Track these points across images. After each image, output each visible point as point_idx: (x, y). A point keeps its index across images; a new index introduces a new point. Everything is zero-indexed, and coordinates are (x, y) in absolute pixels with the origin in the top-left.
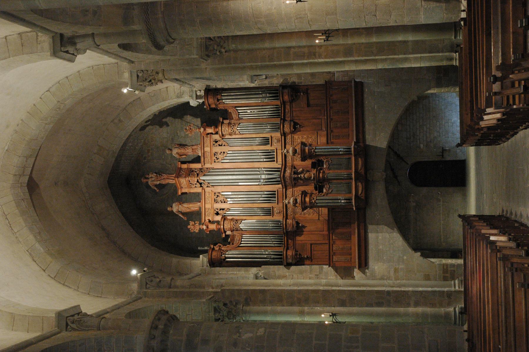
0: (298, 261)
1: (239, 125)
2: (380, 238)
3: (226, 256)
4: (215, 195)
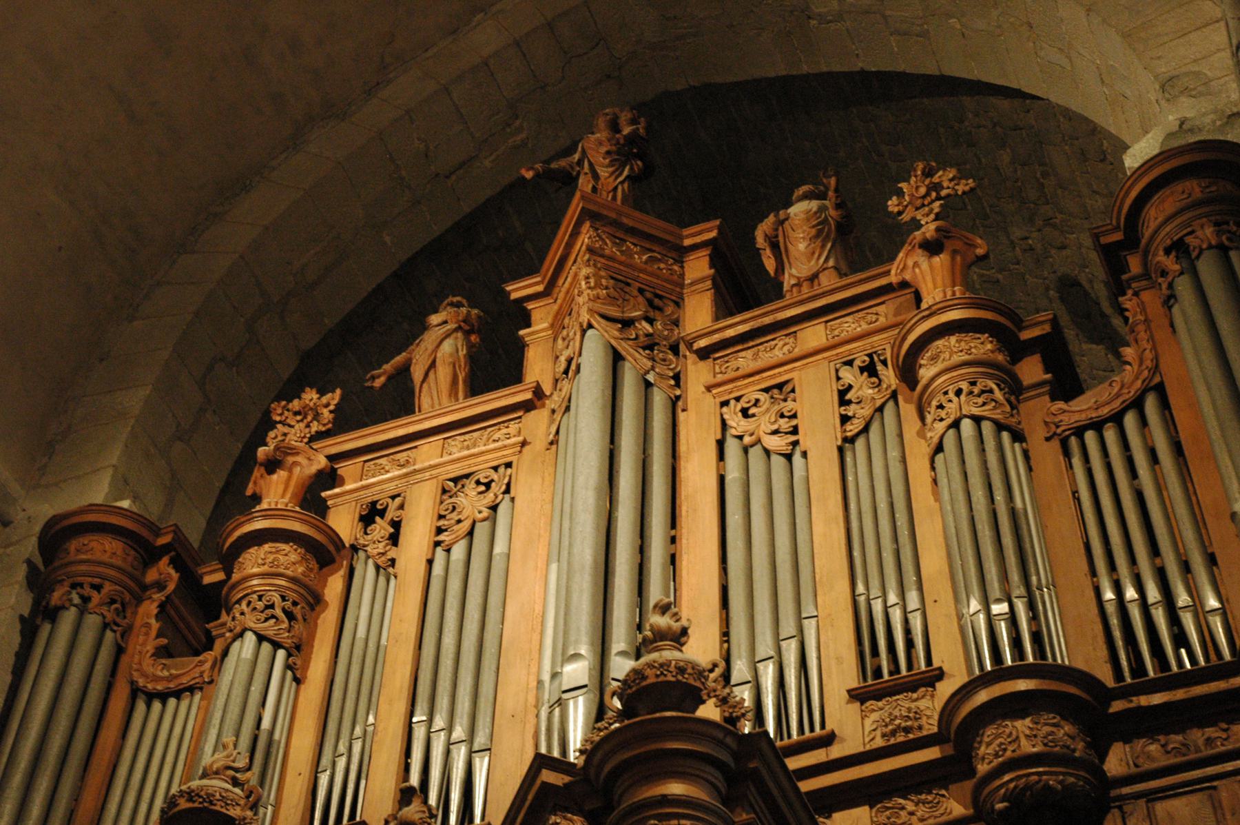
1: (1000, 427)
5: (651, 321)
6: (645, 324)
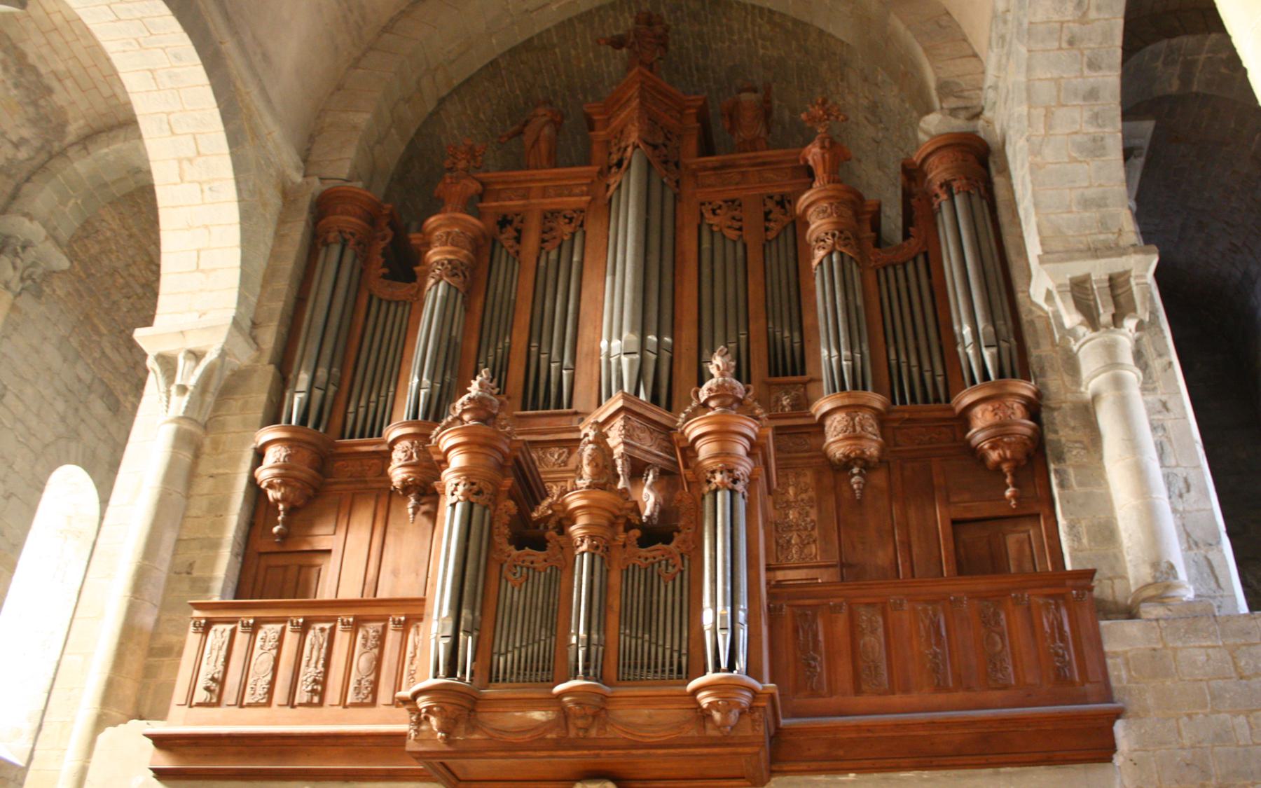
5: (665, 146)
6: (663, 148)
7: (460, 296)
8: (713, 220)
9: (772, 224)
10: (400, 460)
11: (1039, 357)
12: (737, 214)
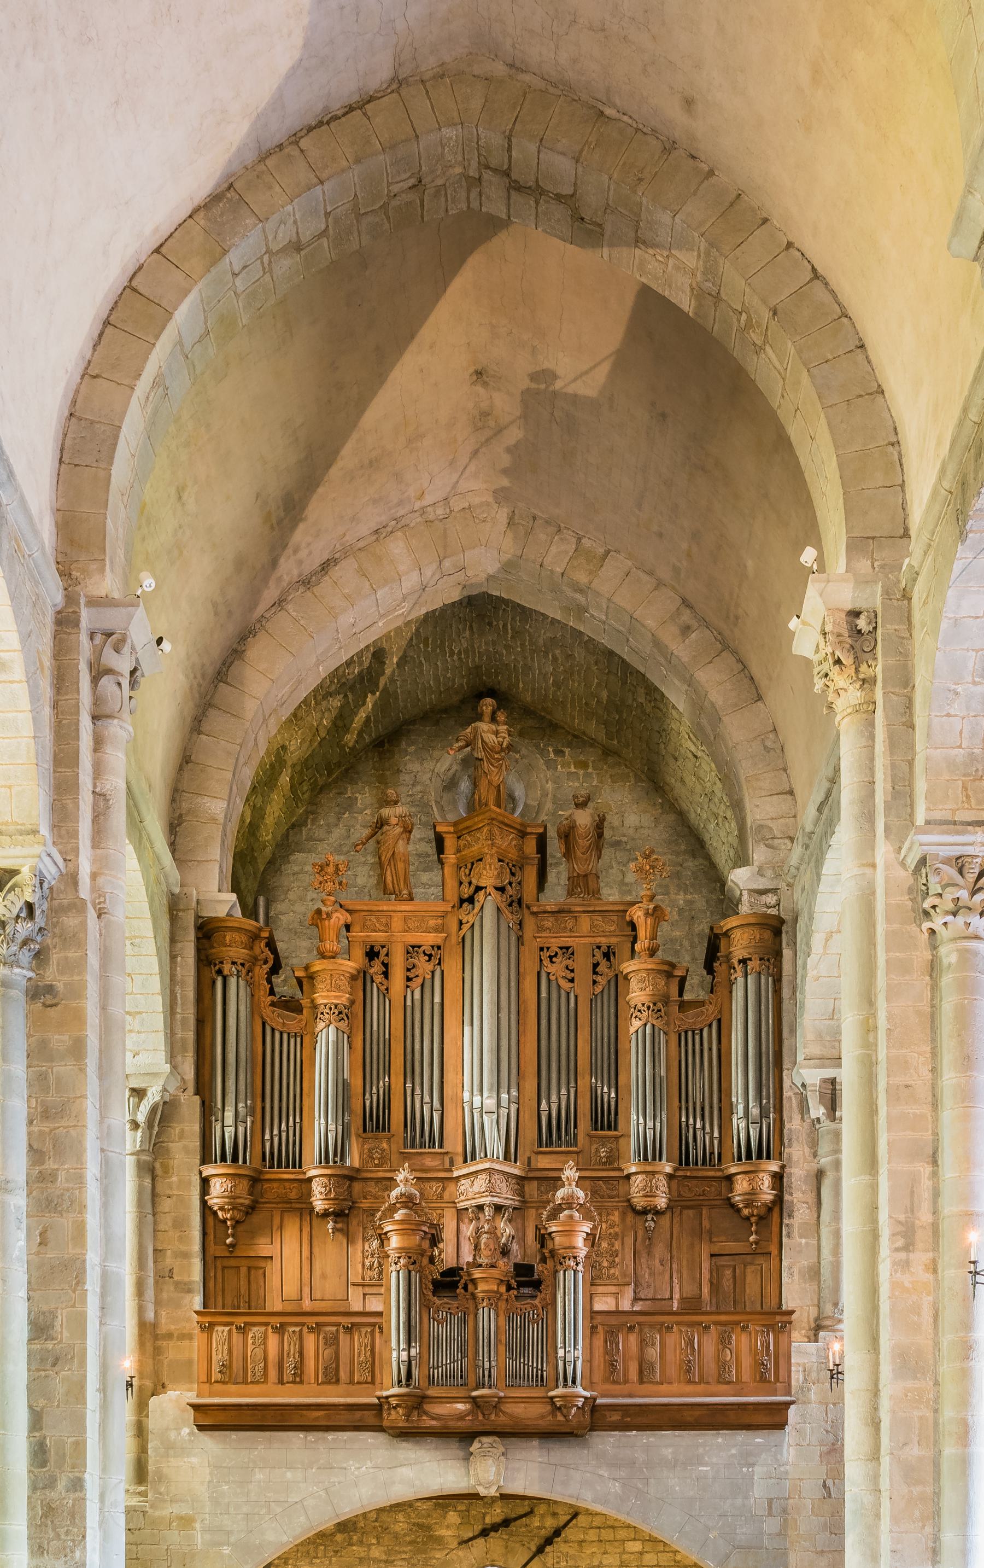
0: (215, 1213)
2: (289, 1475)
3: (233, 981)
4: (433, 947)
7: (346, 1036)
8: (552, 968)
9: (599, 978)
10: (321, 1193)
11: (790, 1130)
12: (569, 962)
